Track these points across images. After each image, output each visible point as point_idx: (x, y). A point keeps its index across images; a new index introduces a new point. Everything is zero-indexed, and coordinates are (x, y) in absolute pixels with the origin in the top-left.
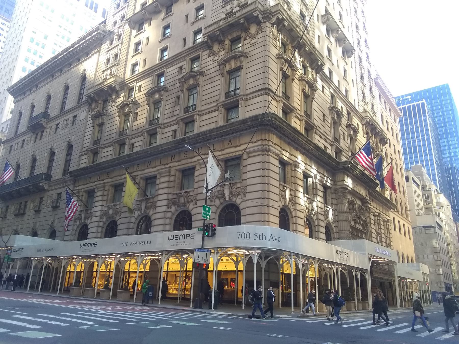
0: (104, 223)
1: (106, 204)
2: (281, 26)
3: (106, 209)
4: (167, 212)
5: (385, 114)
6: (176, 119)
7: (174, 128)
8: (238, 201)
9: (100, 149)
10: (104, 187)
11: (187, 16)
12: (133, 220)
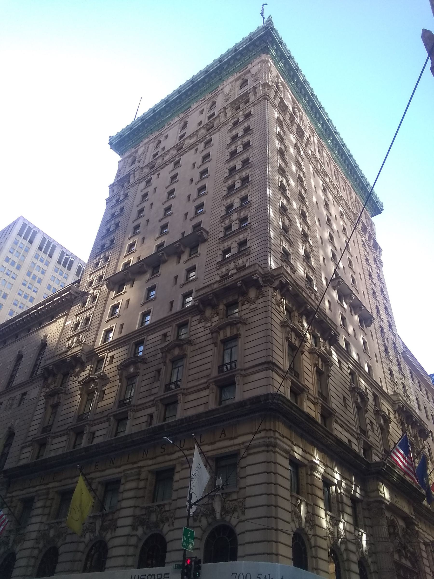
2: (285, 290)
3: (46, 528)
4: (132, 536)
5: (420, 397)
6: (154, 399)
10: (48, 494)
11: (176, 278)
12: (82, 547)
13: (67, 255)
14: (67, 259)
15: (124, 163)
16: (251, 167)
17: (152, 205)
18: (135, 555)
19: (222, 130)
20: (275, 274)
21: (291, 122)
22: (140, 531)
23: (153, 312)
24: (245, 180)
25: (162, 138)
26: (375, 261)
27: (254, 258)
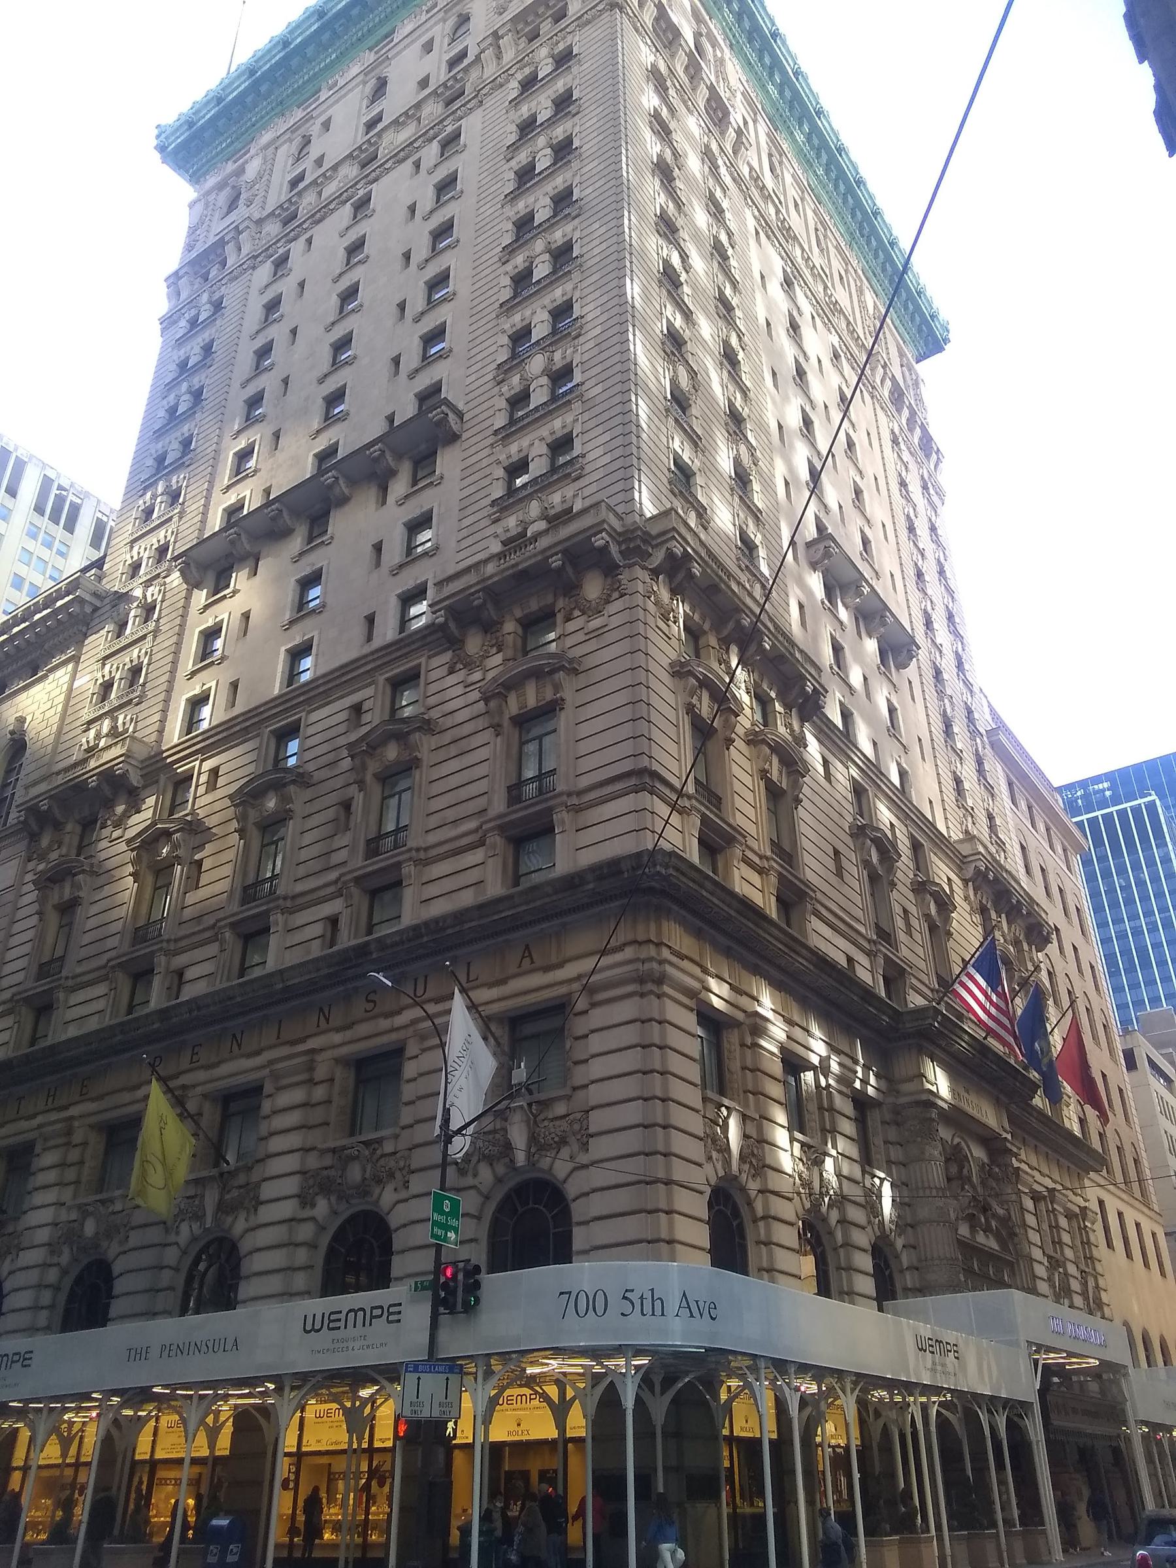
0: (65, 1272)
1: (75, 1197)
2: (681, 576)
3: (74, 1216)
6: (338, 879)
7: (328, 909)
9: (61, 995)
10: (69, 1132)
11: (378, 548)
12: (171, 1256)
13: (60, 488)
14: (60, 501)
15: (207, 205)
16: (578, 215)
17: (294, 332)
18: (311, 1267)
19: (489, 102)
20: (654, 532)
21: (692, 78)
22: (322, 1207)
24: (562, 255)
25: (315, 128)
26: (925, 487)
27: (593, 488)
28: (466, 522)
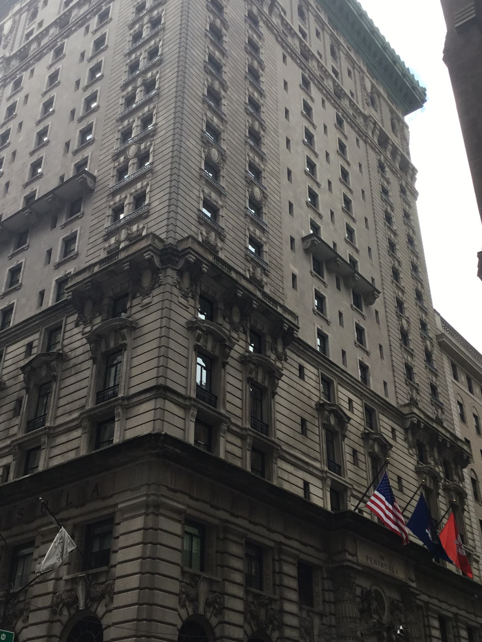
8: (101, 610)
17: (21, 125)
23: (16, 307)
27: (153, 223)
28: (92, 240)
